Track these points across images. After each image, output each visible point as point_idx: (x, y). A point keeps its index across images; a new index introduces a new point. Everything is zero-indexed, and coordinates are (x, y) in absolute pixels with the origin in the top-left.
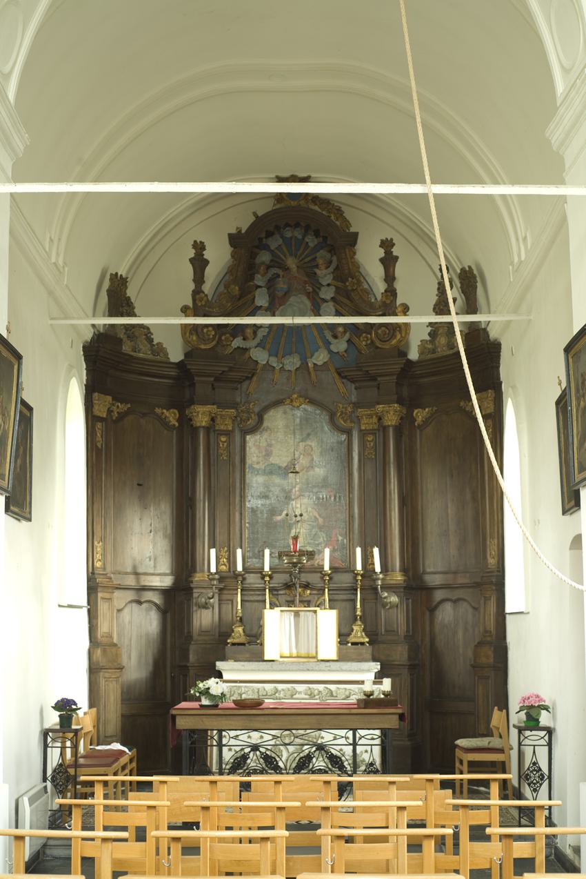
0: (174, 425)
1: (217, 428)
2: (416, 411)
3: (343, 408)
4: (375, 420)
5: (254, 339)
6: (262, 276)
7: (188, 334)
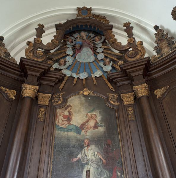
0: (12, 98)
1: (39, 103)
2: (155, 92)
3: (112, 95)
4: (132, 98)
5: (64, 65)
6: (71, 43)
7: (28, 53)
